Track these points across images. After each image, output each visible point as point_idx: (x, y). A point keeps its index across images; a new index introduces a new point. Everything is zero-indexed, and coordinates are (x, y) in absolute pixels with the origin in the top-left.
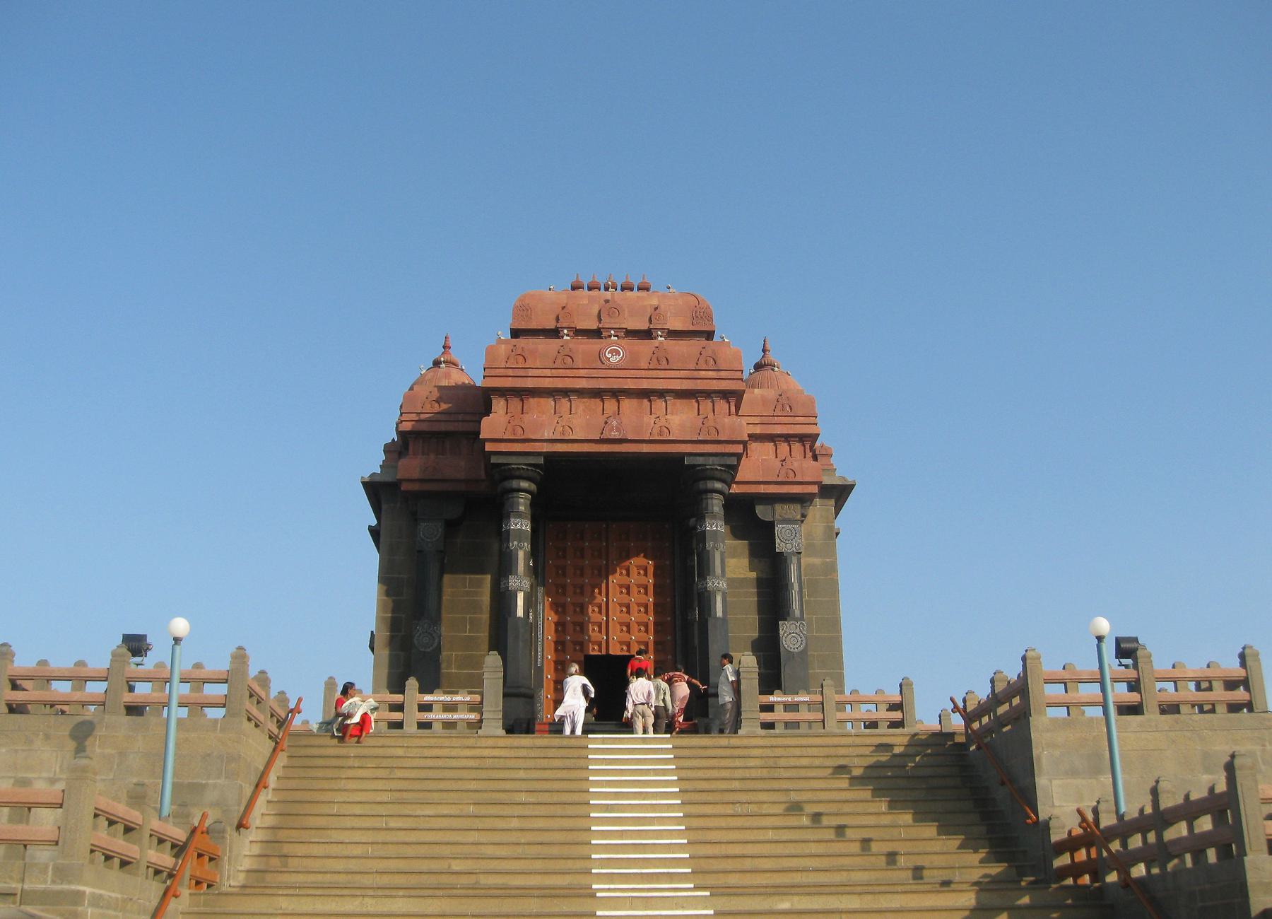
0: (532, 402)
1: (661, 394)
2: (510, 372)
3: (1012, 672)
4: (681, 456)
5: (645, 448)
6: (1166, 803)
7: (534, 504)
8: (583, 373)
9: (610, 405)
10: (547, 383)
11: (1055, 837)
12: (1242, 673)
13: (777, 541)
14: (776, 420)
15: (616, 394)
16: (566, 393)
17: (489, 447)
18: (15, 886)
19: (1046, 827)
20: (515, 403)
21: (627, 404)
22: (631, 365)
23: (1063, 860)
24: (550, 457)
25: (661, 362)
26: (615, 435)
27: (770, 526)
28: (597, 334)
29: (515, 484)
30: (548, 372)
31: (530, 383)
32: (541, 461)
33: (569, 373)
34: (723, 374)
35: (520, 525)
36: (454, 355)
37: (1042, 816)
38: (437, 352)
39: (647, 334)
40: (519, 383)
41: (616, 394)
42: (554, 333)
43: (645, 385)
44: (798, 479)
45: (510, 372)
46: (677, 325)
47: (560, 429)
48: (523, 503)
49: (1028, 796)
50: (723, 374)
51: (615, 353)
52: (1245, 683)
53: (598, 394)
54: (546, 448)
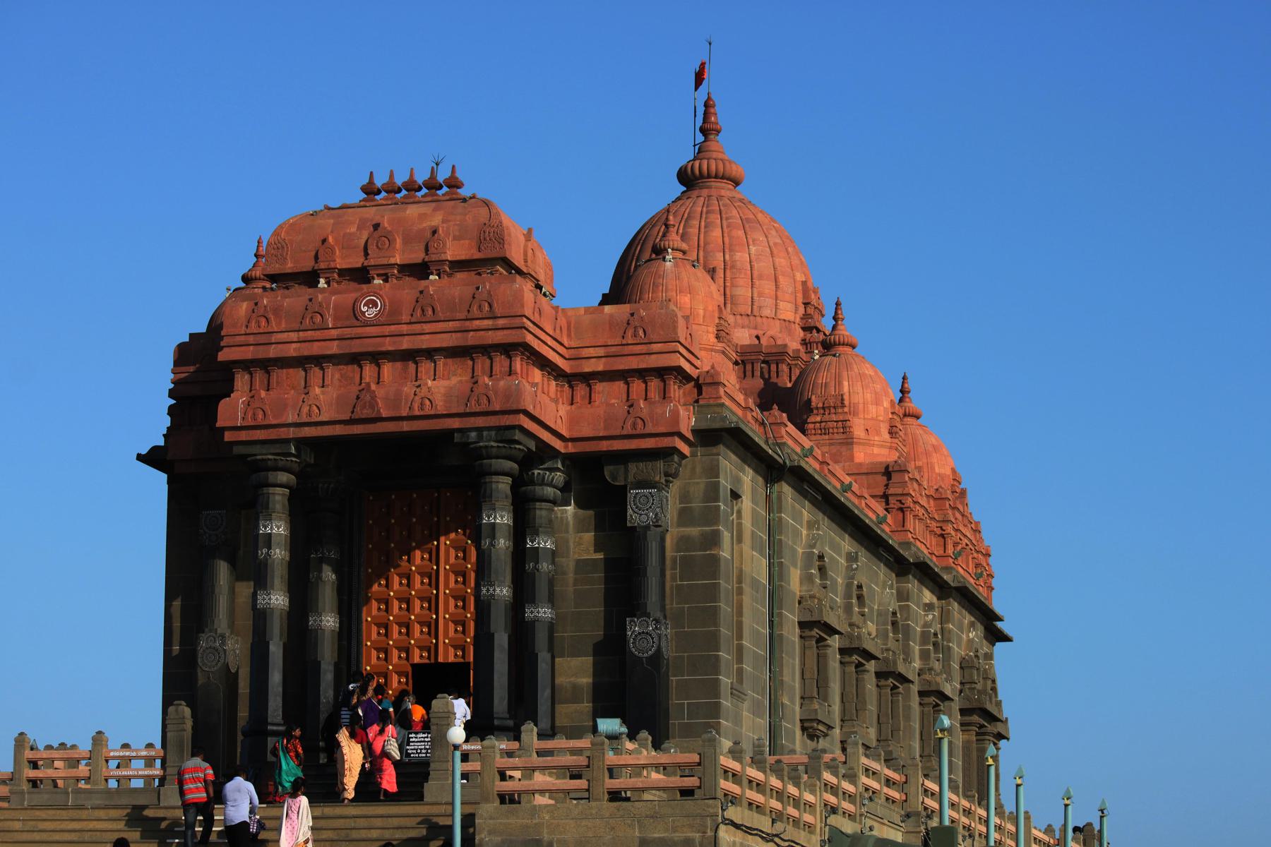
0: (279, 374)
1: (430, 354)
2: (251, 339)
4: (450, 433)
5: (406, 426)
7: (291, 499)
13: (630, 511)
14: (627, 350)
15: (377, 357)
17: (228, 436)
21: (387, 369)
22: (390, 317)
27: (623, 490)
30: (294, 336)
31: (273, 352)
33: (317, 335)
34: (501, 322)
40: (262, 353)
41: (377, 357)
43: (406, 344)
44: (650, 429)
45: (251, 339)
47: (305, 409)
48: (279, 497)
50: (501, 322)
53: (355, 359)
54: (292, 433)
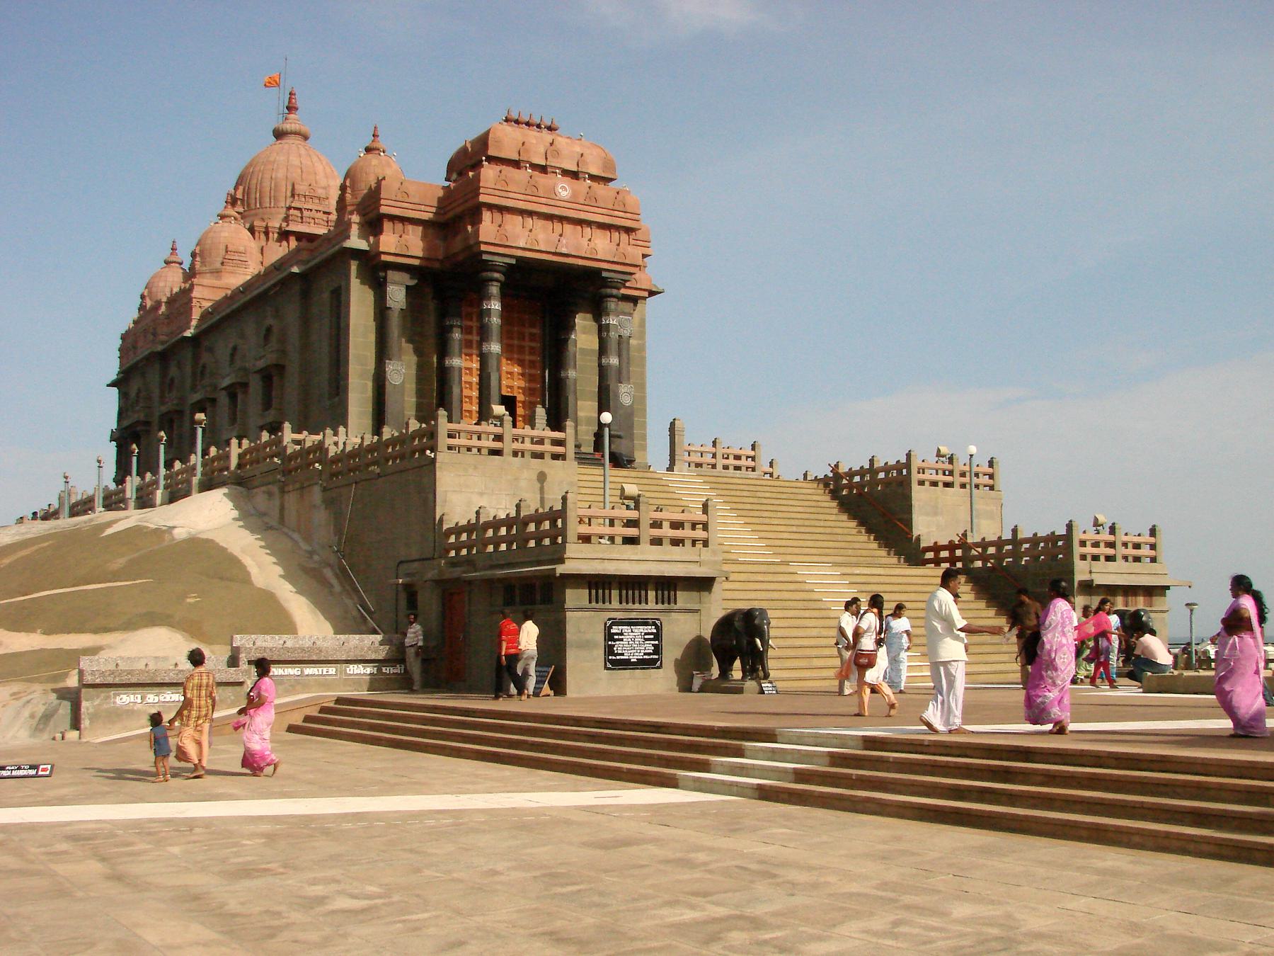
2: (497, 193)
3: (889, 456)
4: (600, 270)
6: (1020, 536)
8: (543, 201)
9: (558, 226)
10: (522, 205)
11: (923, 545)
12: (990, 470)
15: (562, 219)
16: (531, 214)
17: (483, 248)
18: (697, 559)
19: (918, 539)
20: (497, 216)
21: (568, 228)
23: (930, 555)
24: (519, 259)
25: (592, 201)
26: (564, 251)
28: (543, 169)
29: (489, 274)
32: (513, 261)
33: (534, 199)
34: (629, 215)
35: (495, 305)
36: (381, 143)
37: (915, 533)
38: (368, 141)
39: (575, 175)
41: (562, 219)
42: (516, 164)
43: (582, 216)
45: (497, 193)
46: (594, 172)
48: (494, 289)
49: (909, 523)
50: (629, 215)
51: (564, 189)
52: (991, 476)
54: (519, 253)
